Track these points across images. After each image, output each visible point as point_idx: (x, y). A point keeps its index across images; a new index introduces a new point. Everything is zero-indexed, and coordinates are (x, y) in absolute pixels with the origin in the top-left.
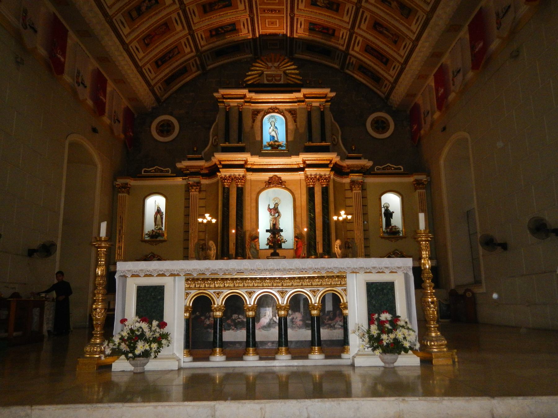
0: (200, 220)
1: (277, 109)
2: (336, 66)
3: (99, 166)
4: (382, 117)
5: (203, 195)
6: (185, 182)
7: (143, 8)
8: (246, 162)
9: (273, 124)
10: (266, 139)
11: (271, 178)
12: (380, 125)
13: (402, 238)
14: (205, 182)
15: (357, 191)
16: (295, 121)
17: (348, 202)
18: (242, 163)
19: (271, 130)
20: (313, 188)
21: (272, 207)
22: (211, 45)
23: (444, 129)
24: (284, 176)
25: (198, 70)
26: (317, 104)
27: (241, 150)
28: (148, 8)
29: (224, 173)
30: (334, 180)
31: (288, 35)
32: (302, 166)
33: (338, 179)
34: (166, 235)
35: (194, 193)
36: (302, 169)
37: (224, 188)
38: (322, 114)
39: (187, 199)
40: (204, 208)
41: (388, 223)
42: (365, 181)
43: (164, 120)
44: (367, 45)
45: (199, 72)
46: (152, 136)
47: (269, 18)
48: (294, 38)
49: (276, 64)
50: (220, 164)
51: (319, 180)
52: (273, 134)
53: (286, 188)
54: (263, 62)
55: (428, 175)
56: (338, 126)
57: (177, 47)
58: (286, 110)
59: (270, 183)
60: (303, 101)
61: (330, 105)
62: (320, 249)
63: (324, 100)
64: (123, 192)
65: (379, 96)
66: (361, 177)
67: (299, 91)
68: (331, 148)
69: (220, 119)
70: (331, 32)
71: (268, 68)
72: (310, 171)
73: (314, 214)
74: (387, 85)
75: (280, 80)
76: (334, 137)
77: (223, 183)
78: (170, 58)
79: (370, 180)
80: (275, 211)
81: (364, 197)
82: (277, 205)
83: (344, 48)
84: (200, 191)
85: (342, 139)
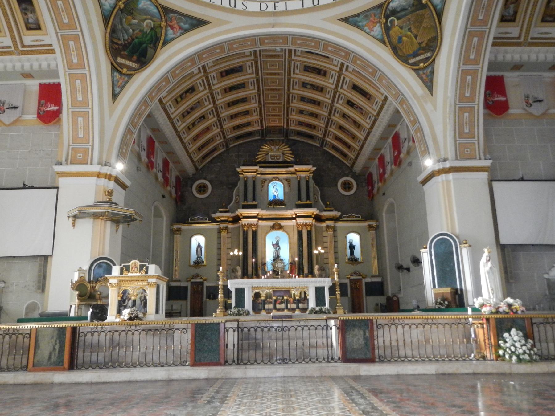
0: (231, 254)
1: (277, 178)
2: (318, 145)
3: (165, 218)
4: (348, 181)
5: (230, 235)
6: (217, 227)
7: (196, 123)
8: (258, 215)
9: (275, 187)
11: (274, 224)
12: (347, 186)
13: (360, 263)
14: (230, 226)
15: (331, 232)
16: (290, 186)
17: (325, 239)
18: (256, 215)
19: (273, 191)
20: (302, 231)
21: (275, 243)
22: (234, 135)
23: (384, 194)
24: (283, 223)
25: (224, 147)
26: (304, 176)
27: (255, 207)
28: (199, 122)
29: (244, 221)
30: (315, 225)
31: (285, 127)
32: (294, 216)
33: (318, 224)
34: (205, 262)
35: (224, 234)
36: (294, 219)
37: (244, 231)
38: (308, 182)
39: (219, 238)
40: (230, 244)
41: (352, 253)
43: (201, 183)
44: (336, 136)
45: (224, 149)
46: (193, 195)
47: (272, 118)
48: (288, 129)
49: (277, 147)
50: (241, 215)
51: (305, 225)
52: (275, 194)
53: (284, 231)
54: (268, 145)
55: (377, 221)
56: (318, 189)
57: (212, 138)
58: (284, 179)
59: (273, 228)
60: (295, 173)
61: (313, 176)
62: (306, 271)
63: (308, 173)
64: (177, 234)
65: (347, 165)
66: (333, 223)
67: (292, 167)
68: (313, 205)
69: (241, 185)
70: (313, 127)
71: (272, 150)
72: (300, 220)
73: (303, 249)
74: (371, 117)
75: (279, 159)
76: (315, 196)
77: (243, 229)
78: (207, 144)
80: (277, 246)
81: (335, 236)
82: (278, 241)
83: (321, 136)
84: (228, 233)
85: (321, 197)
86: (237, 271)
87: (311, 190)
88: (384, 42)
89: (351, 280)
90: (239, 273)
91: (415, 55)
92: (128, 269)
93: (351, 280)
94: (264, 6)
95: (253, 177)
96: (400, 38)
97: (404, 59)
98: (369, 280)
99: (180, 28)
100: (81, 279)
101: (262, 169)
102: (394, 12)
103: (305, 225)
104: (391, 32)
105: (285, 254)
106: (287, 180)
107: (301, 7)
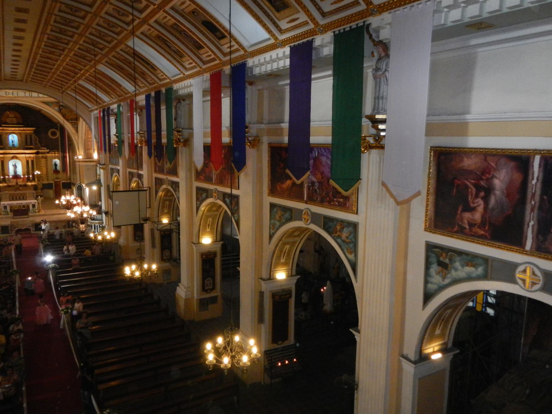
10: (11, 143)
15: (44, 160)
16: (21, 137)
17: (41, 162)
24: (17, 155)
33: (37, 156)
38: (31, 136)
41: (56, 168)
42: (47, 156)
52: (13, 139)
59: (13, 158)
62: (31, 179)
79: (48, 155)
80: (15, 166)
81: (46, 161)
82: (15, 164)
87: (33, 139)
88: (59, 112)
91: (71, 120)
93: (55, 182)
94: (7, 93)
97: (68, 120)
98: (63, 181)
101: (5, 128)
102: (62, 106)
103: (30, 157)
104: (62, 111)
105: (20, 171)
107: (24, 96)
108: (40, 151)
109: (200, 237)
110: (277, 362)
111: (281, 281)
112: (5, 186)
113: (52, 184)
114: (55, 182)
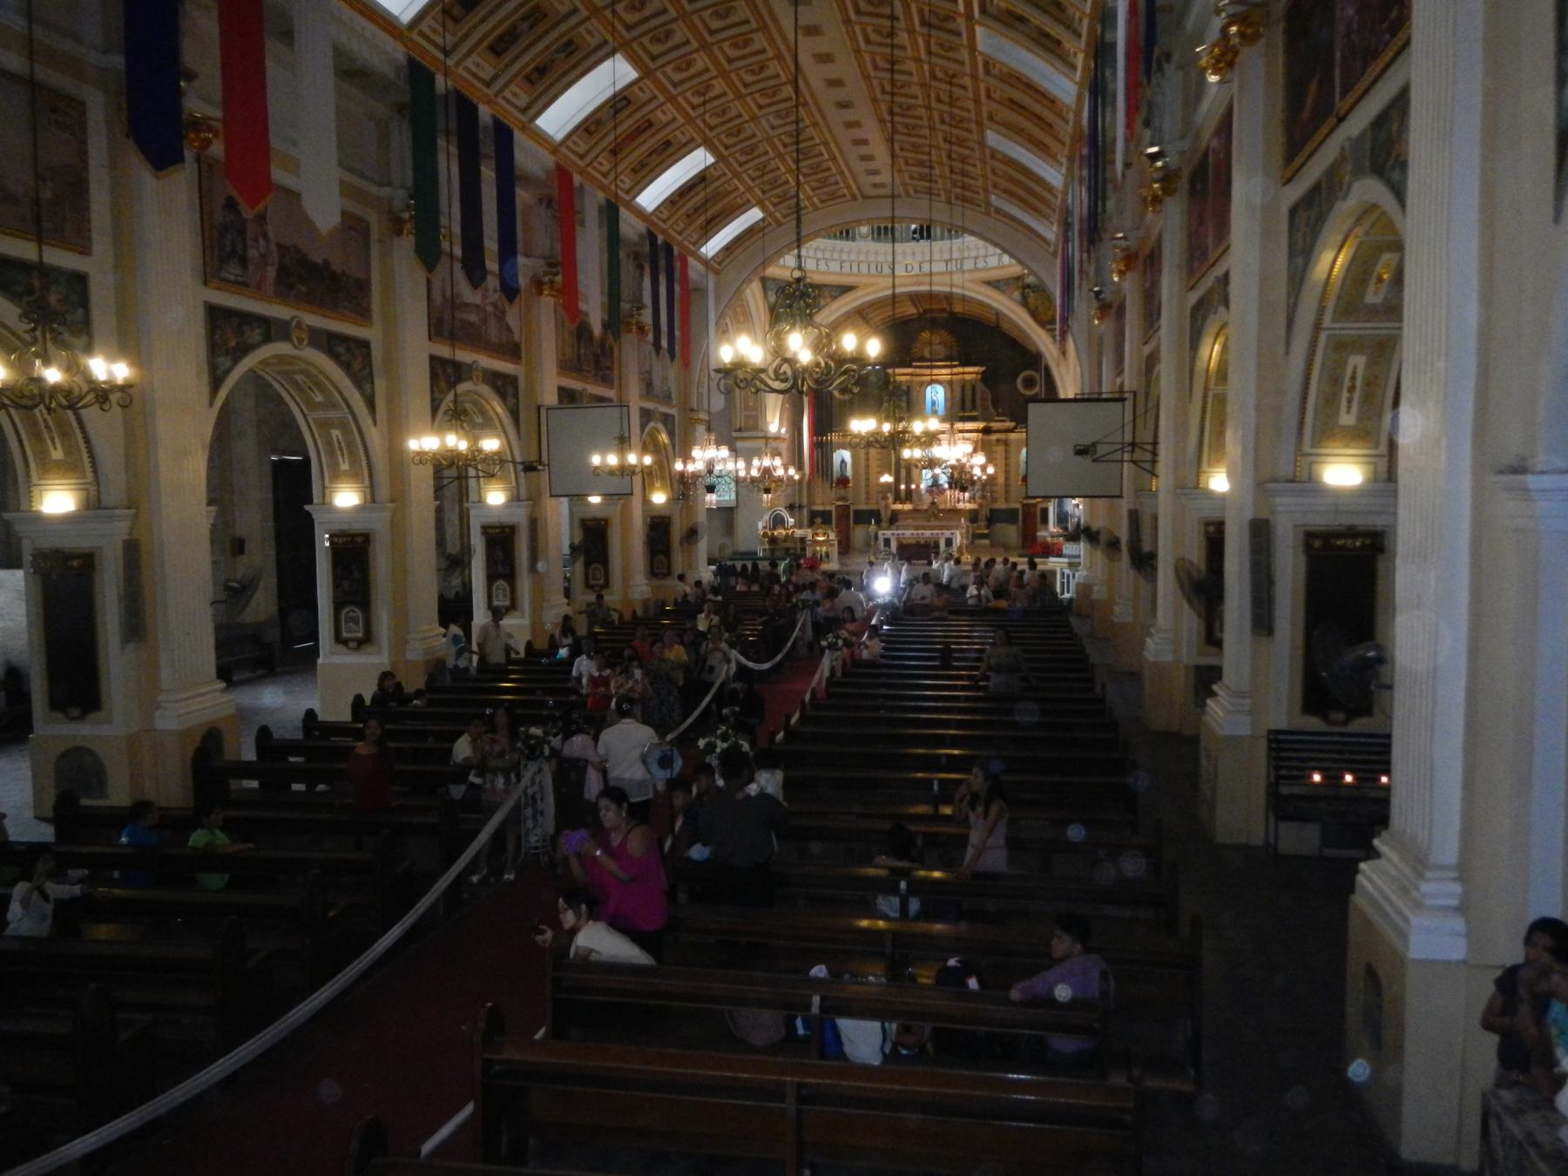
16: (952, 390)
33: (986, 437)
79: (1012, 436)
81: (1006, 451)
86: (887, 498)
87: (978, 396)
89: (1024, 505)
90: (891, 499)
92: (817, 535)
93: (1024, 505)
94: (909, 268)
95: (907, 381)
96: (1036, 308)
99: (831, 296)
100: (765, 527)
101: (918, 371)
102: (1028, 286)
106: (951, 383)
108: (995, 425)
109: (1205, 467)
110: (1308, 772)
111: (1338, 494)
112: (910, 511)
113: (1015, 511)
114: (1024, 505)
